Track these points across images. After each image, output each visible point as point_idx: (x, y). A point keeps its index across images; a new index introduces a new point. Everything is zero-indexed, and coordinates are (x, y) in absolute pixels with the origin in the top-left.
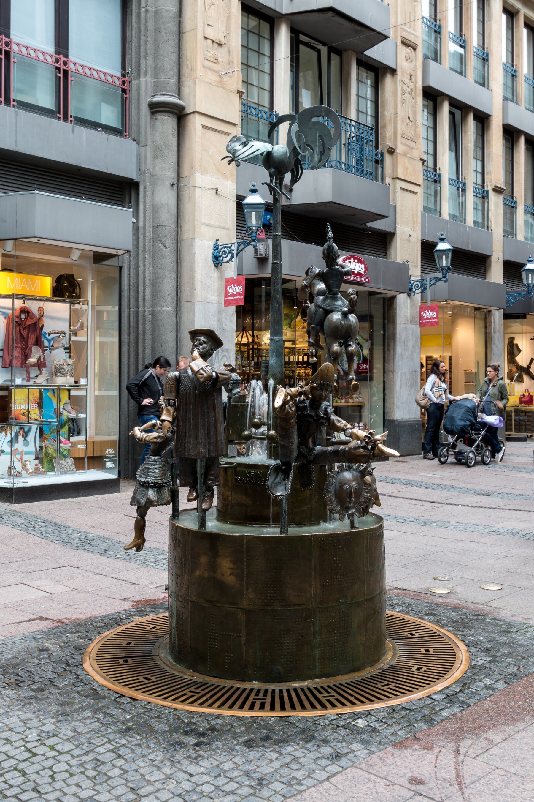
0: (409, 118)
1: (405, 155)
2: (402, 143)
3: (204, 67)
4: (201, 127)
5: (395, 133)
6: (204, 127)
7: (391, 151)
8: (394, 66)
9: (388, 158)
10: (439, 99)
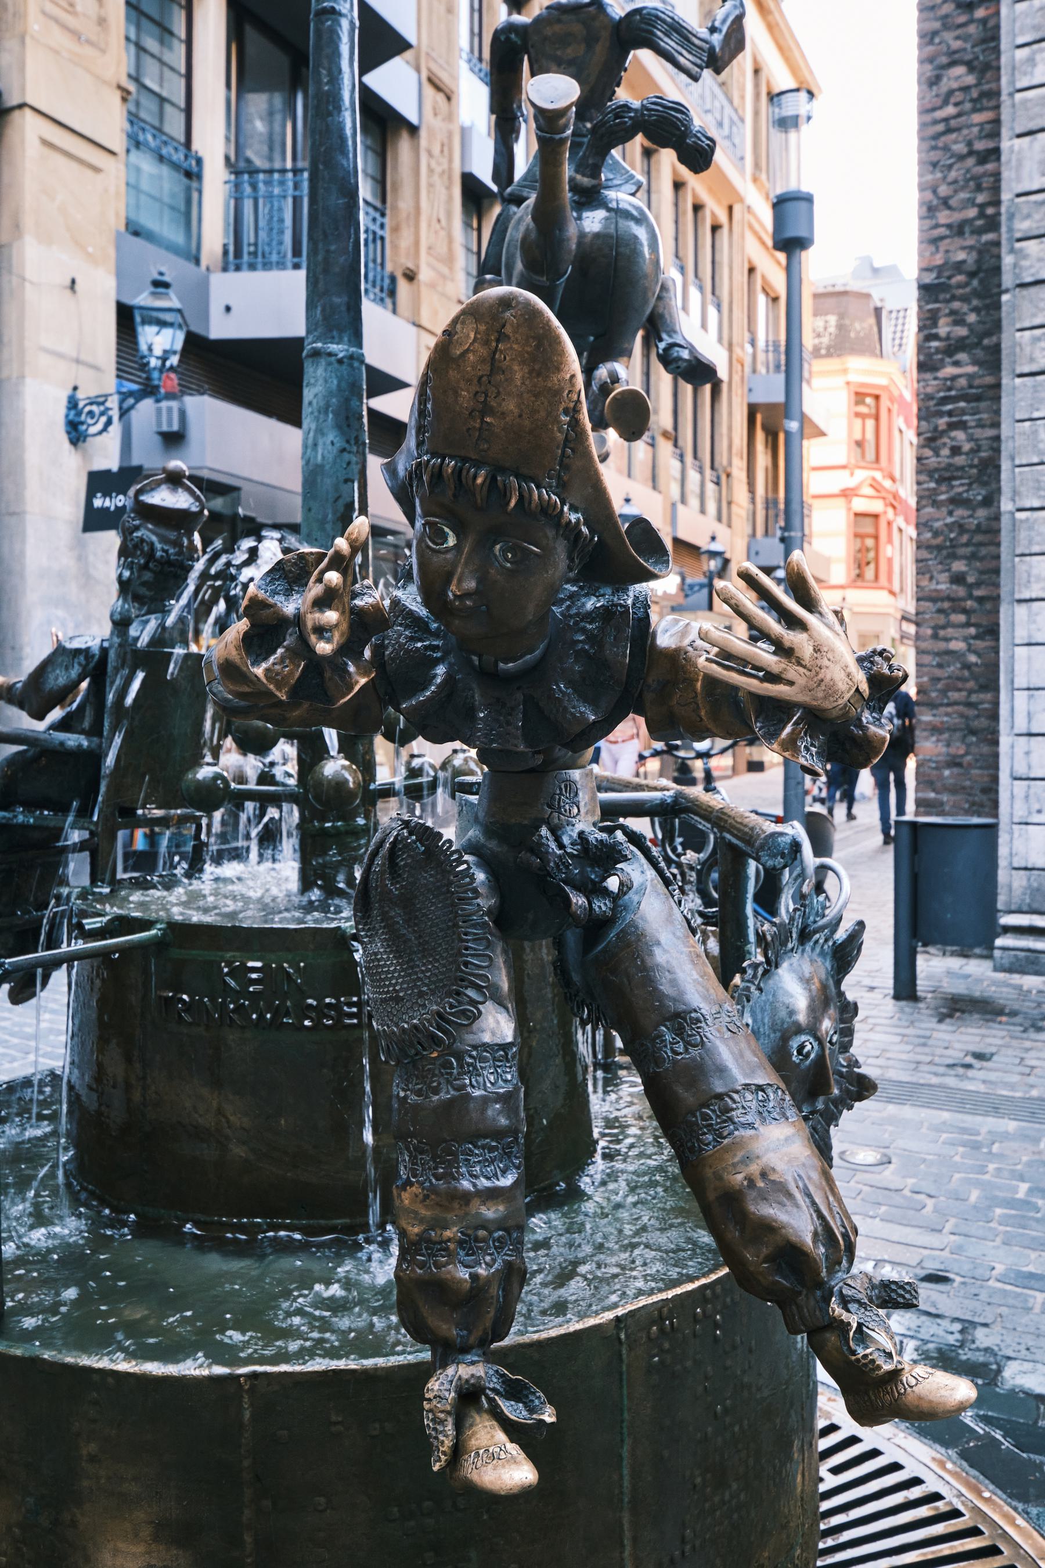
0: (439, 221)
1: (432, 286)
2: (429, 265)
3: (44, 13)
4: (37, 142)
5: (417, 243)
6: (45, 143)
7: (410, 276)
8: (413, 119)
9: (402, 285)
10: (486, 202)
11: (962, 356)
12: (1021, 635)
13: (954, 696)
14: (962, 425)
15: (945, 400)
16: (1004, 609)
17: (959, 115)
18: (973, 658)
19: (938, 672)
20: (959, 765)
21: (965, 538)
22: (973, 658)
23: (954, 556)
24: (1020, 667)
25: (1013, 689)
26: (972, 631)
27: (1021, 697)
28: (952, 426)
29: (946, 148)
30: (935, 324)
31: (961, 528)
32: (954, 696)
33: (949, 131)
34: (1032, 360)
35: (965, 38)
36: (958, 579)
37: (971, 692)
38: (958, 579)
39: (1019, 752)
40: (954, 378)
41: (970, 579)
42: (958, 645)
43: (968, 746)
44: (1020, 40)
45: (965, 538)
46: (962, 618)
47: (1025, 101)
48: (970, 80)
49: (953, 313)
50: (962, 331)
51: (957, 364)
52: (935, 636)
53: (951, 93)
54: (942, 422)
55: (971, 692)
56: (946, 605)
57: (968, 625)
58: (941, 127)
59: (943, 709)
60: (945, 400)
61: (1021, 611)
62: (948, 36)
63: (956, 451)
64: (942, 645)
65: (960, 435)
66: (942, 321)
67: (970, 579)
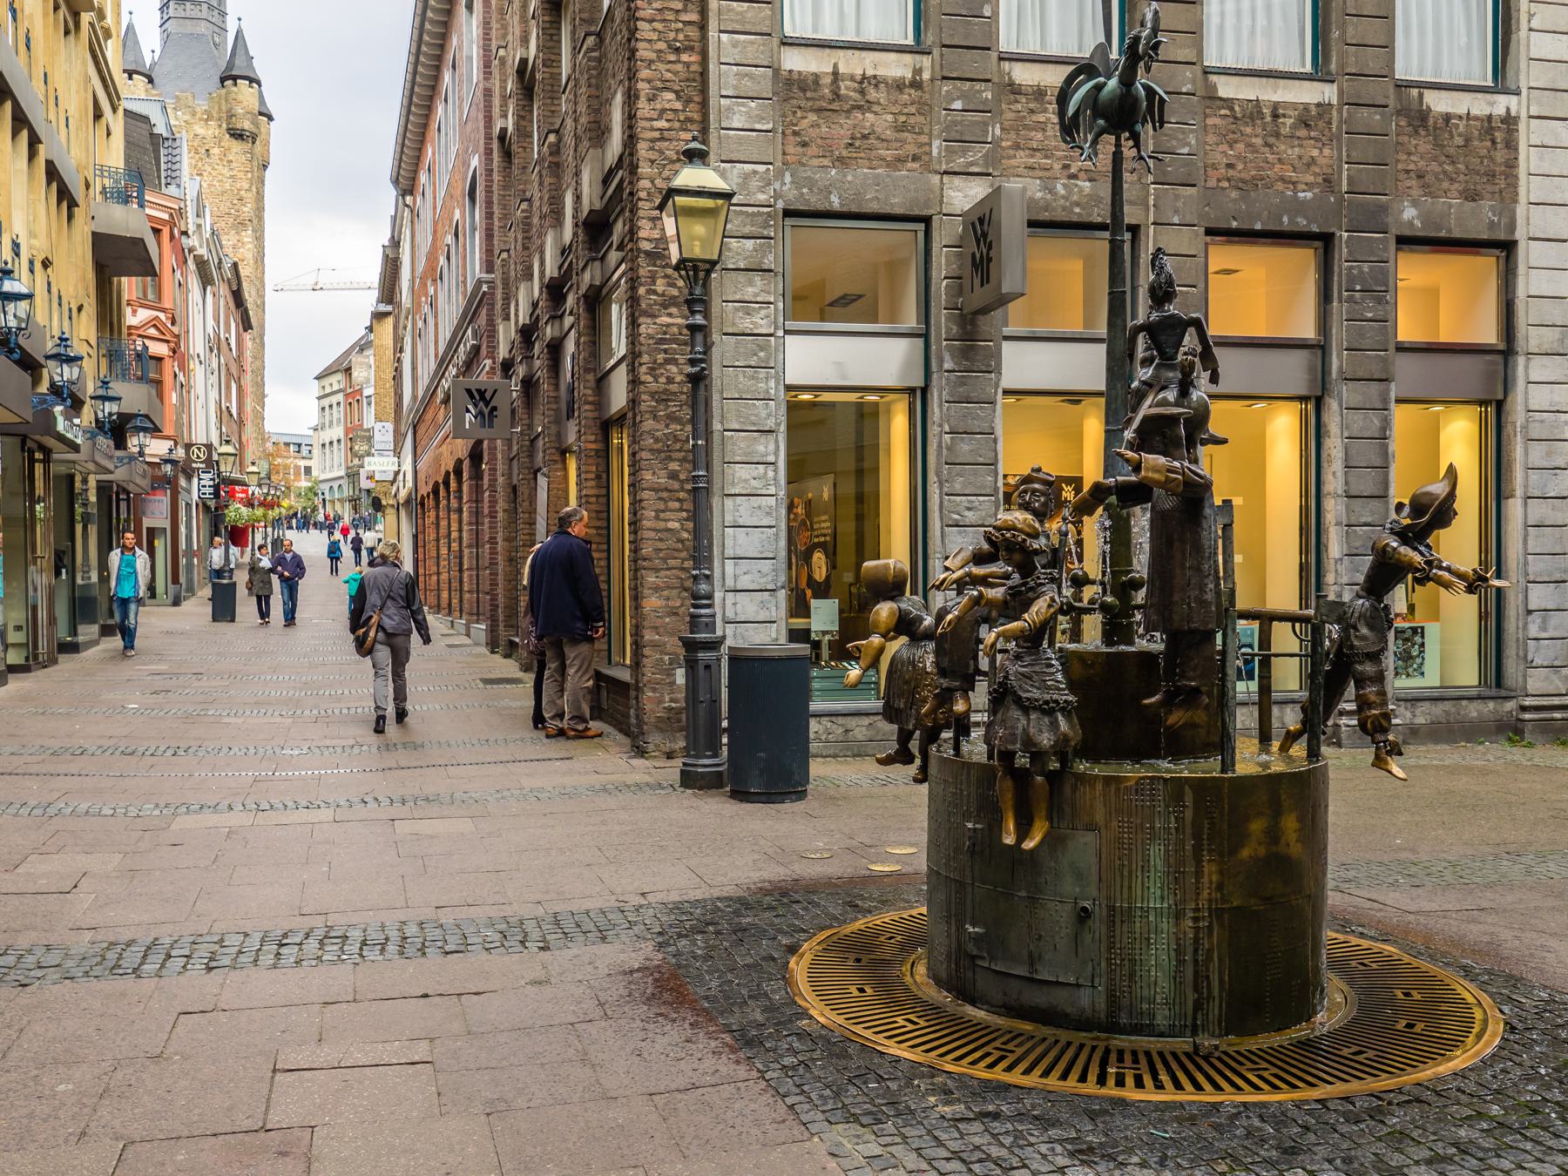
11: (674, 310)
12: (729, 519)
13: (672, 562)
14: (675, 362)
15: (662, 341)
16: (716, 501)
17: (669, 130)
18: (685, 535)
19: (660, 545)
20: (676, 614)
21: (678, 446)
22: (685, 535)
23: (670, 459)
24: (729, 542)
25: (724, 558)
26: (684, 514)
27: (729, 564)
28: (667, 362)
29: (661, 152)
30: (654, 283)
31: (676, 439)
32: (672, 562)
33: (662, 139)
34: (734, 324)
35: (675, 73)
36: (673, 476)
37: (684, 560)
38: (673, 476)
39: (729, 603)
40: (668, 325)
41: (682, 477)
42: (675, 525)
43: (683, 599)
44: (724, 93)
45: (678, 446)
46: (677, 505)
47: (729, 137)
48: (678, 105)
49: (666, 276)
50: (675, 292)
51: (670, 315)
52: (657, 518)
53: (664, 111)
54: (661, 357)
55: (684, 560)
56: (665, 495)
57: (681, 510)
58: (657, 134)
59: (663, 573)
60: (662, 341)
61: (729, 502)
62: (662, 67)
63: (670, 380)
64: (662, 525)
65: (674, 369)
66: (659, 281)
67: (682, 477)
